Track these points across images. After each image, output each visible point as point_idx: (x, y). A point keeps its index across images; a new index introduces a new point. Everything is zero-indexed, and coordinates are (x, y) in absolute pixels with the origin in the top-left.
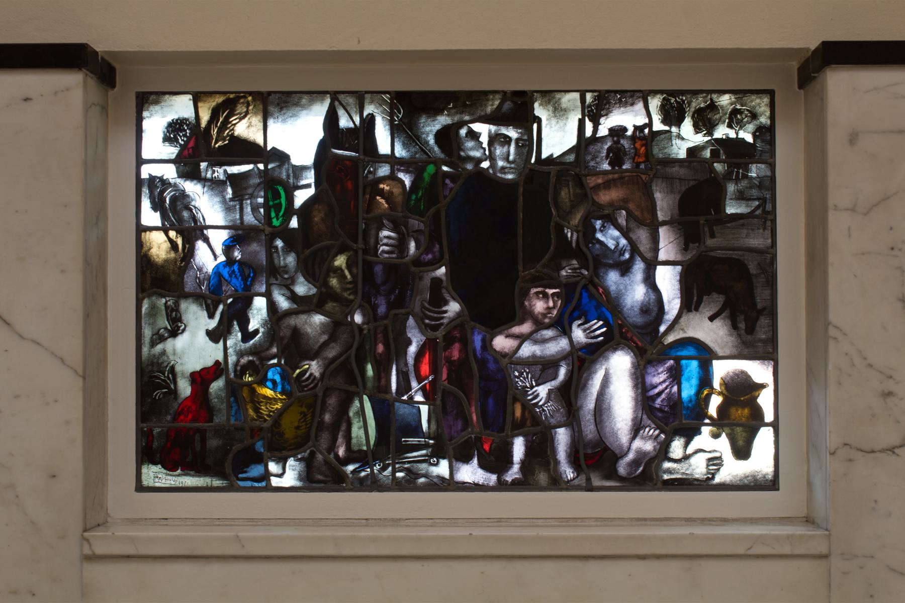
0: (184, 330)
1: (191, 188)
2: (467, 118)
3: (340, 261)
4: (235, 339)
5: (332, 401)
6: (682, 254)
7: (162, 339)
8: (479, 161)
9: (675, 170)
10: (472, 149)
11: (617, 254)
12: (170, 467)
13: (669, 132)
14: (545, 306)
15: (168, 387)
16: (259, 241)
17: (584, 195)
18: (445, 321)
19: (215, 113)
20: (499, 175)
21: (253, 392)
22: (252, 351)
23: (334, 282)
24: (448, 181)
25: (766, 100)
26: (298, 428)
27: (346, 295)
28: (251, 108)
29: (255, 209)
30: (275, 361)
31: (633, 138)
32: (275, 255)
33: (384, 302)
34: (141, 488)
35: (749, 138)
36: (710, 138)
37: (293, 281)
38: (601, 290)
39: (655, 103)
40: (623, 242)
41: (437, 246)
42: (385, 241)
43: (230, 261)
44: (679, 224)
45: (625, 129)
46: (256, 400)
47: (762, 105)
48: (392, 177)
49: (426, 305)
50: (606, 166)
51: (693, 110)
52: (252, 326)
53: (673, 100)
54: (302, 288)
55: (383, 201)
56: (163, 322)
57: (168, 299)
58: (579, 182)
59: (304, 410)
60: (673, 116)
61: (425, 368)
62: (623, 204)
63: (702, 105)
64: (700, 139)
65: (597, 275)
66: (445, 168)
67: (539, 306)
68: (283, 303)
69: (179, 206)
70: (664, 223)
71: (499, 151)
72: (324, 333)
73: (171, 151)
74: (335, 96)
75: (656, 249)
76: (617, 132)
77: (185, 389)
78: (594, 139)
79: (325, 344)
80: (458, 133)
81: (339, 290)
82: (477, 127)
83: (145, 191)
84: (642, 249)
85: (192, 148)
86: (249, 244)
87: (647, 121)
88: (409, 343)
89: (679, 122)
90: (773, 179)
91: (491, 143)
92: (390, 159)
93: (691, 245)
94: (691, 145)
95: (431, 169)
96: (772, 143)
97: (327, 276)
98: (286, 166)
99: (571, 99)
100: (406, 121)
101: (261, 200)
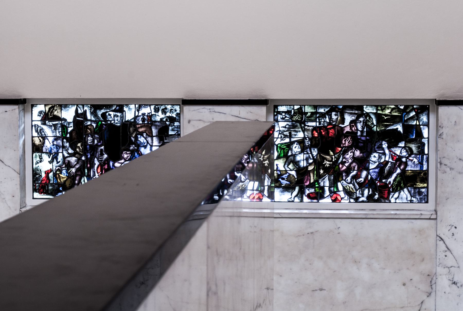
0: (43, 161)
1: (44, 127)
2: (108, 111)
3: (79, 145)
4: (55, 162)
5: (77, 178)
6: (159, 144)
7: (38, 163)
8: (111, 121)
9: (157, 123)
10: (109, 118)
11: (143, 144)
12: (41, 193)
13: (156, 114)
14: (127, 156)
15: (39, 174)
16: (60, 140)
17: (136, 130)
18: (104, 159)
19: (50, 109)
20: (116, 124)
21: (59, 176)
22: (59, 166)
23: (78, 150)
24: (104, 126)
25: (179, 107)
26: (70, 184)
27: (80, 153)
28: (58, 108)
29: (59, 132)
30: (64, 168)
31: (147, 116)
32: (64, 143)
33: (89, 154)
34: (33, 198)
35: (175, 116)
36: (165, 116)
37: (68, 149)
38: (140, 152)
39: (152, 107)
40: (145, 141)
41: (102, 141)
42: (90, 140)
43: (54, 145)
44: (158, 136)
45: (145, 114)
46: (60, 178)
47: (177, 108)
48: (91, 125)
49: (99, 155)
50: (141, 122)
51: (161, 109)
52: (59, 161)
53: (157, 107)
54: (71, 151)
55: (89, 130)
56: (38, 159)
57: (39, 153)
58: (135, 126)
59: (71, 180)
60: (157, 110)
61: (99, 171)
62: (145, 132)
63: (164, 108)
64: (163, 116)
65: (139, 149)
66: (103, 123)
67: (125, 156)
68: (66, 155)
69: (42, 131)
70: (155, 136)
71: (116, 118)
72: (75, 162)
73: (40, 118)
74: (77, 105)
75: (152, 143)
76: (144, 114)
77: (43, 175)
78: (138, 116)
79: (76, 165)
80: (106, 114)
81: (79, 152)
82: (111, 113)
83: (34, 128)
84: (149, 142)
85: (44, 118)
86: (58, 141)
87: (151, 112)
88: (95, 164)
89: (158, 111)
90: (180, 126)
91: (114, 117)
92: (91, 121)
93: (161, 142)
94: (161, 117)
95: (100, 123)
96: (180, 117)
97: (76, 148)
98: (66, 122)
99: (132, 106)
100: (94, 111)
101: (60, 130)
